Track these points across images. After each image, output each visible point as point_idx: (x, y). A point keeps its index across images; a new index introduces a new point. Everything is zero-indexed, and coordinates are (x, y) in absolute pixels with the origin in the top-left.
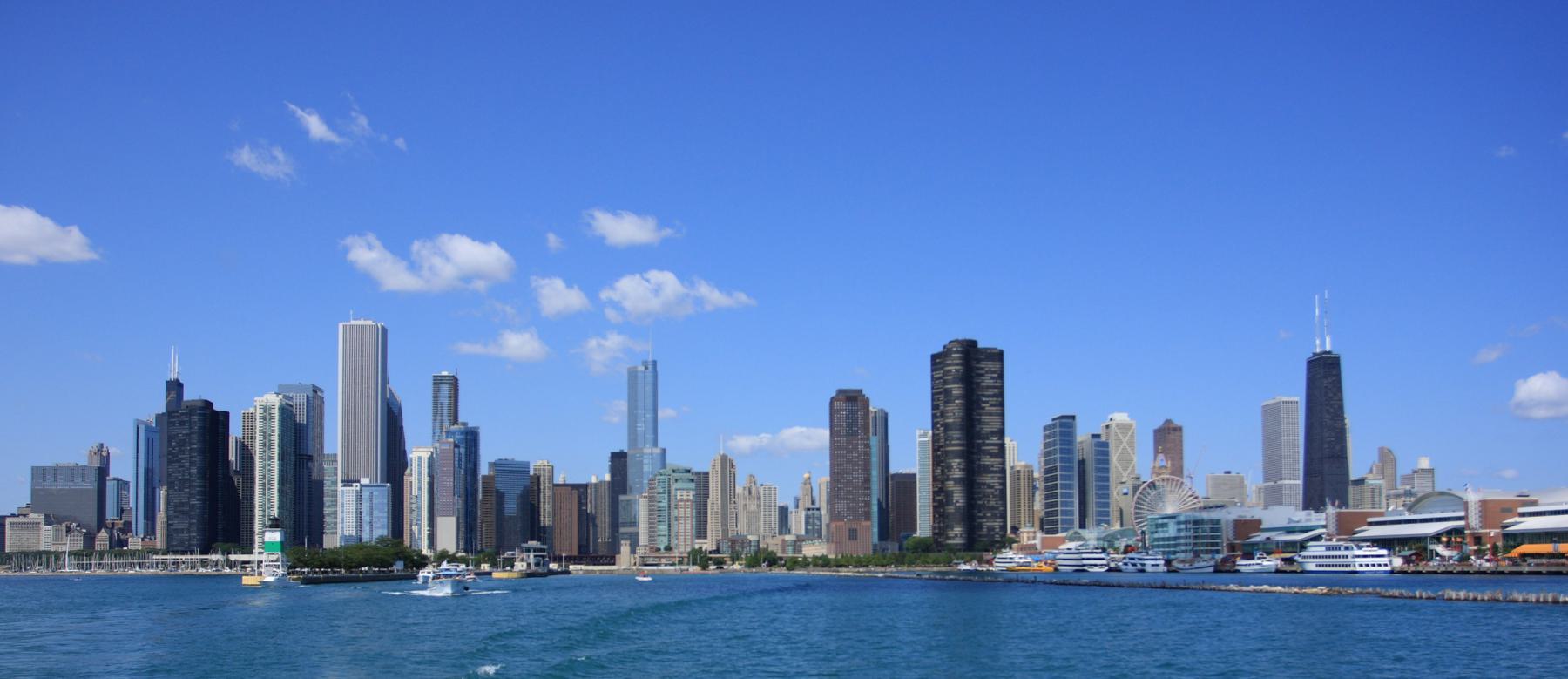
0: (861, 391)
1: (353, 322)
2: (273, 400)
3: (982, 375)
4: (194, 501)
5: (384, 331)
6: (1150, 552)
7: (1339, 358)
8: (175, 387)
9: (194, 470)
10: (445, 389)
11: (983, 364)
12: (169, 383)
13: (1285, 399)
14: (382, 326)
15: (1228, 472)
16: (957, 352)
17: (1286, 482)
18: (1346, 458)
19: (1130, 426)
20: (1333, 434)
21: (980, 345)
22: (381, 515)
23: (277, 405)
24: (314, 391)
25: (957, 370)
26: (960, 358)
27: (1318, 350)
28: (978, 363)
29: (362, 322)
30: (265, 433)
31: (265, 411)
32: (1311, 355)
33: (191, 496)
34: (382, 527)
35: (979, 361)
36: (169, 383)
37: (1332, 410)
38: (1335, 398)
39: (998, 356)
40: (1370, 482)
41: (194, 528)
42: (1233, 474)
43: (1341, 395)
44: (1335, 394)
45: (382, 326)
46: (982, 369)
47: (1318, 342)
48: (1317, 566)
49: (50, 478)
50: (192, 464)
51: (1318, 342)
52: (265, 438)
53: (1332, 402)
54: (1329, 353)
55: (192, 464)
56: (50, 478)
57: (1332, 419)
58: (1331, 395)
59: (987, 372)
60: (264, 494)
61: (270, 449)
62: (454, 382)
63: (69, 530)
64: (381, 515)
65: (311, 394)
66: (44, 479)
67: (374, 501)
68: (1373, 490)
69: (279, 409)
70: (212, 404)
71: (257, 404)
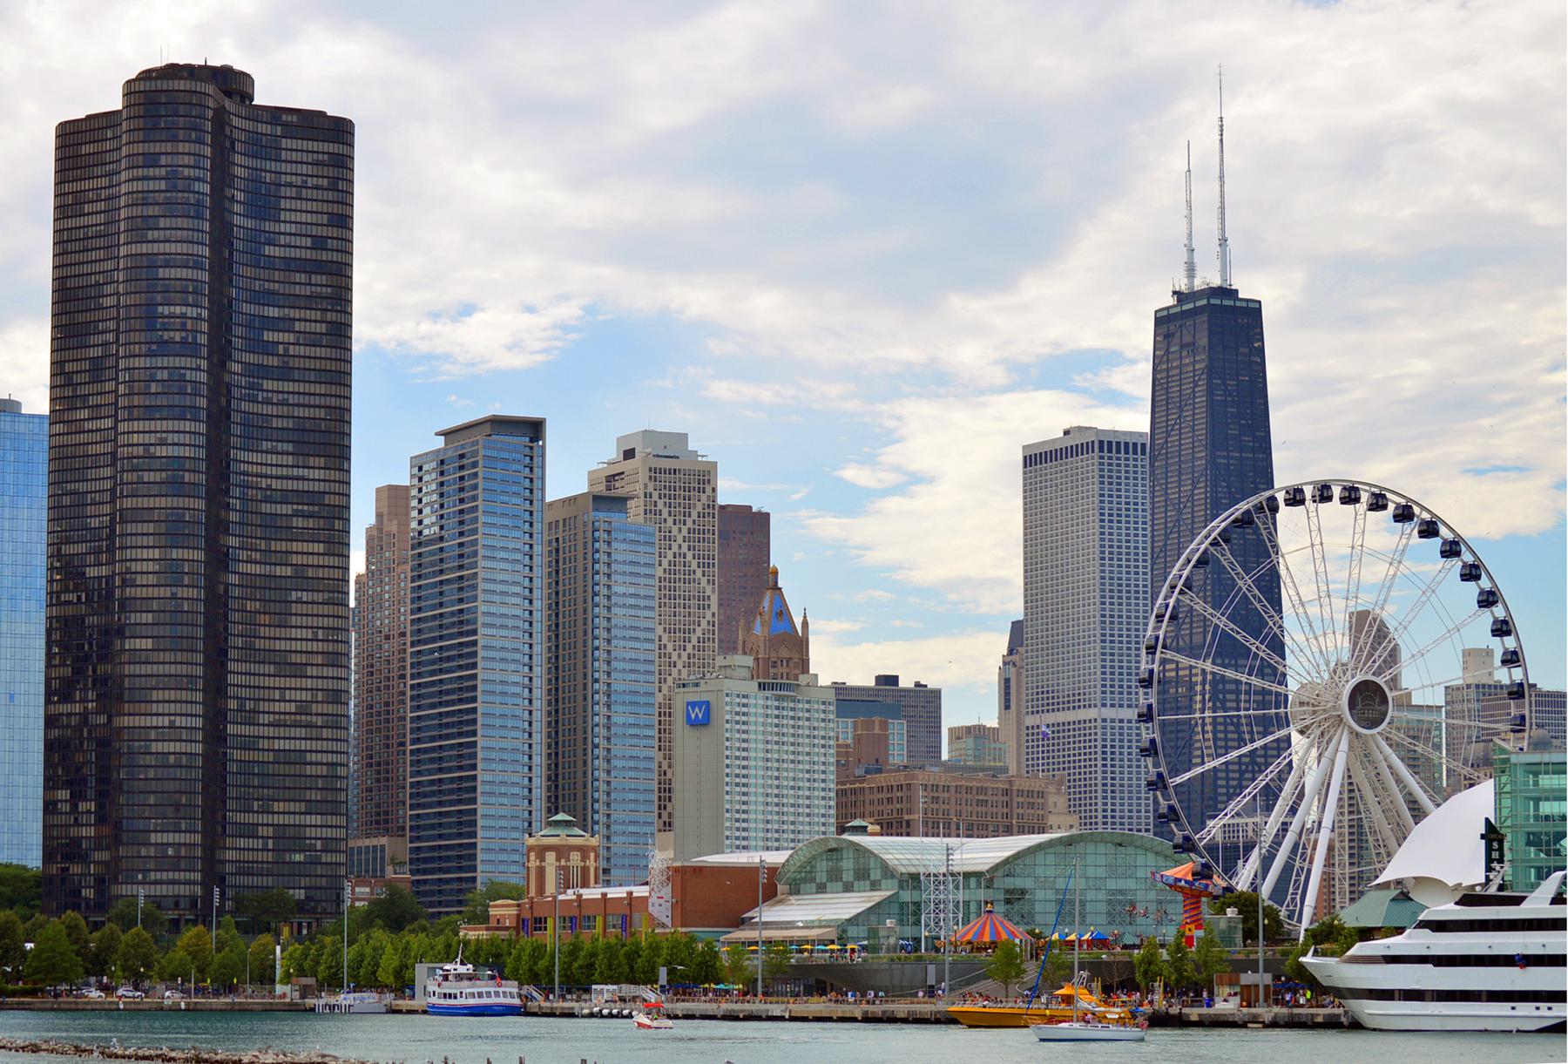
7: (1259, 311)
42: (904, 683)
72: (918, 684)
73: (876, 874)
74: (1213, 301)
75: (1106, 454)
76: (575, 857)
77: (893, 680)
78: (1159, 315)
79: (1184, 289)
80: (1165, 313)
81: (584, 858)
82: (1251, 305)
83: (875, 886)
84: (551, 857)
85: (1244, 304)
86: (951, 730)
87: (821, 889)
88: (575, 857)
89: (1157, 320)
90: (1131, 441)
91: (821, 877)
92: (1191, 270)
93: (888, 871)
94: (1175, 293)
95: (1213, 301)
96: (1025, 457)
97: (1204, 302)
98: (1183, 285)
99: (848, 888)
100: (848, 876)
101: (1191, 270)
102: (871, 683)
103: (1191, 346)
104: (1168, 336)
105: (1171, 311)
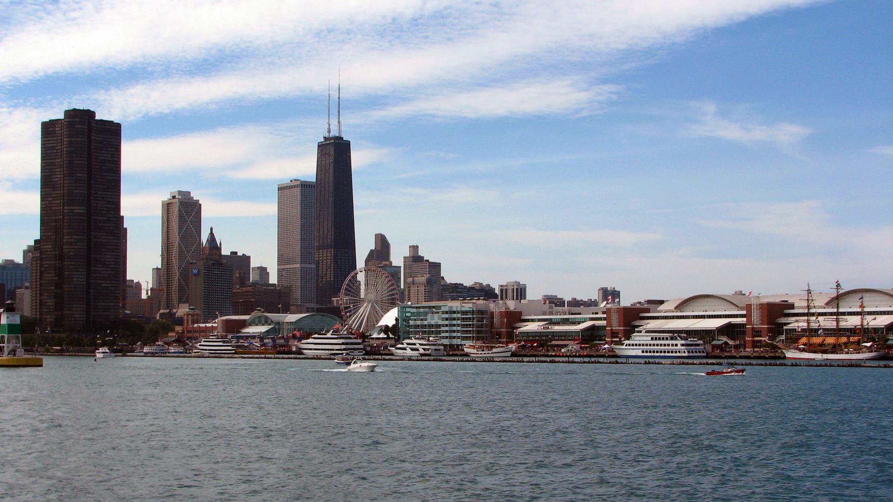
6: (431, 339)
48: (643, 352)
72: (243, 254)
73: (269, 322)
74: (336, 141)
75: (303, 188)
76: (196, 317)
77: (236, 253)
78: (319, 144)
79: (327, 136)
80: (321, 144)
81: (198, 317)
82: (347, 142)
83: (270, 325)
84: (190, 316)
85: (345, 142)
86: (252, 268)
87: (257, 325)
88: (196, 317)
89: (319, 146)
90: (311, 184)
91: (257, 322)
92: (329, 131)
93: (272, 322)
94: (324, 137)
95: (336, 141)
96: (278, 188)
97: (333, 141)
98: (327, 135)
99: (263, 325)
100: (263, 322)
101: (329, 131)
102: (229, 254)
103: (329, 155)
104: (322, 151)
105: (323, 143)
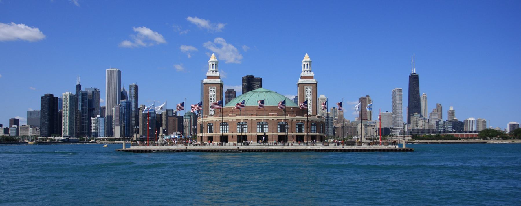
0: (234, 90)
1: (110, 69)
2: (67, 94)
3: (255, 85)
4: (46, 122)
5: (120, 72)
7: (418, 75)
8: (79, 87)
9: (46, 114)
10: (133, 89)
11: (255, 82)
12: (77, 86)
13: (397, 89)
14: (118, 70)
15: (387, 112)
16: (245, 79)
17: (397, 115)
18: (420, 107)
19: (325, 99)
20: (416, 100)
21: (255, 77)
22: (103, 126)
23: (69, 95)
24: (95, 90)
25: (245, 84)
26: (246, 81)
27: (412, 73)
28: (254, 82)
29: (113, 69)
30: (65, 103)
31: (65, 97)
32: (410, 75)
33: (46, 121)
34: (103, 129)
35: (254, 81)
36: (77, 86)
37: (415, 92)
38: (417, 88)
39: (260, 80)
40: (416, 115)
41: (46, 130)
43: (419, 87)
44: (416, 87)
45: (118, 70)
46: (255, 84)
47: (412, 70)
49: (32, 115)
50: (46, 112)
51: (412, 70)
52: (65, 104)
53: (415, 89)
54: (415, 74)
55: (46, 112)
56: (32, 115)
57: (415, 95)
58: (415, 87)
59: (256, 85)
60: (65, 120)
61: (66, 107)
62: (136, 87)
63: (36, 130)
64: (103, 126)
65: (94, 91)
66: (31, 115)
67: (101, 122)
68: (417, 118)
69: (69, 96)
70: (53, 95)
71: (63, 95)
